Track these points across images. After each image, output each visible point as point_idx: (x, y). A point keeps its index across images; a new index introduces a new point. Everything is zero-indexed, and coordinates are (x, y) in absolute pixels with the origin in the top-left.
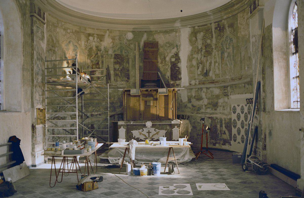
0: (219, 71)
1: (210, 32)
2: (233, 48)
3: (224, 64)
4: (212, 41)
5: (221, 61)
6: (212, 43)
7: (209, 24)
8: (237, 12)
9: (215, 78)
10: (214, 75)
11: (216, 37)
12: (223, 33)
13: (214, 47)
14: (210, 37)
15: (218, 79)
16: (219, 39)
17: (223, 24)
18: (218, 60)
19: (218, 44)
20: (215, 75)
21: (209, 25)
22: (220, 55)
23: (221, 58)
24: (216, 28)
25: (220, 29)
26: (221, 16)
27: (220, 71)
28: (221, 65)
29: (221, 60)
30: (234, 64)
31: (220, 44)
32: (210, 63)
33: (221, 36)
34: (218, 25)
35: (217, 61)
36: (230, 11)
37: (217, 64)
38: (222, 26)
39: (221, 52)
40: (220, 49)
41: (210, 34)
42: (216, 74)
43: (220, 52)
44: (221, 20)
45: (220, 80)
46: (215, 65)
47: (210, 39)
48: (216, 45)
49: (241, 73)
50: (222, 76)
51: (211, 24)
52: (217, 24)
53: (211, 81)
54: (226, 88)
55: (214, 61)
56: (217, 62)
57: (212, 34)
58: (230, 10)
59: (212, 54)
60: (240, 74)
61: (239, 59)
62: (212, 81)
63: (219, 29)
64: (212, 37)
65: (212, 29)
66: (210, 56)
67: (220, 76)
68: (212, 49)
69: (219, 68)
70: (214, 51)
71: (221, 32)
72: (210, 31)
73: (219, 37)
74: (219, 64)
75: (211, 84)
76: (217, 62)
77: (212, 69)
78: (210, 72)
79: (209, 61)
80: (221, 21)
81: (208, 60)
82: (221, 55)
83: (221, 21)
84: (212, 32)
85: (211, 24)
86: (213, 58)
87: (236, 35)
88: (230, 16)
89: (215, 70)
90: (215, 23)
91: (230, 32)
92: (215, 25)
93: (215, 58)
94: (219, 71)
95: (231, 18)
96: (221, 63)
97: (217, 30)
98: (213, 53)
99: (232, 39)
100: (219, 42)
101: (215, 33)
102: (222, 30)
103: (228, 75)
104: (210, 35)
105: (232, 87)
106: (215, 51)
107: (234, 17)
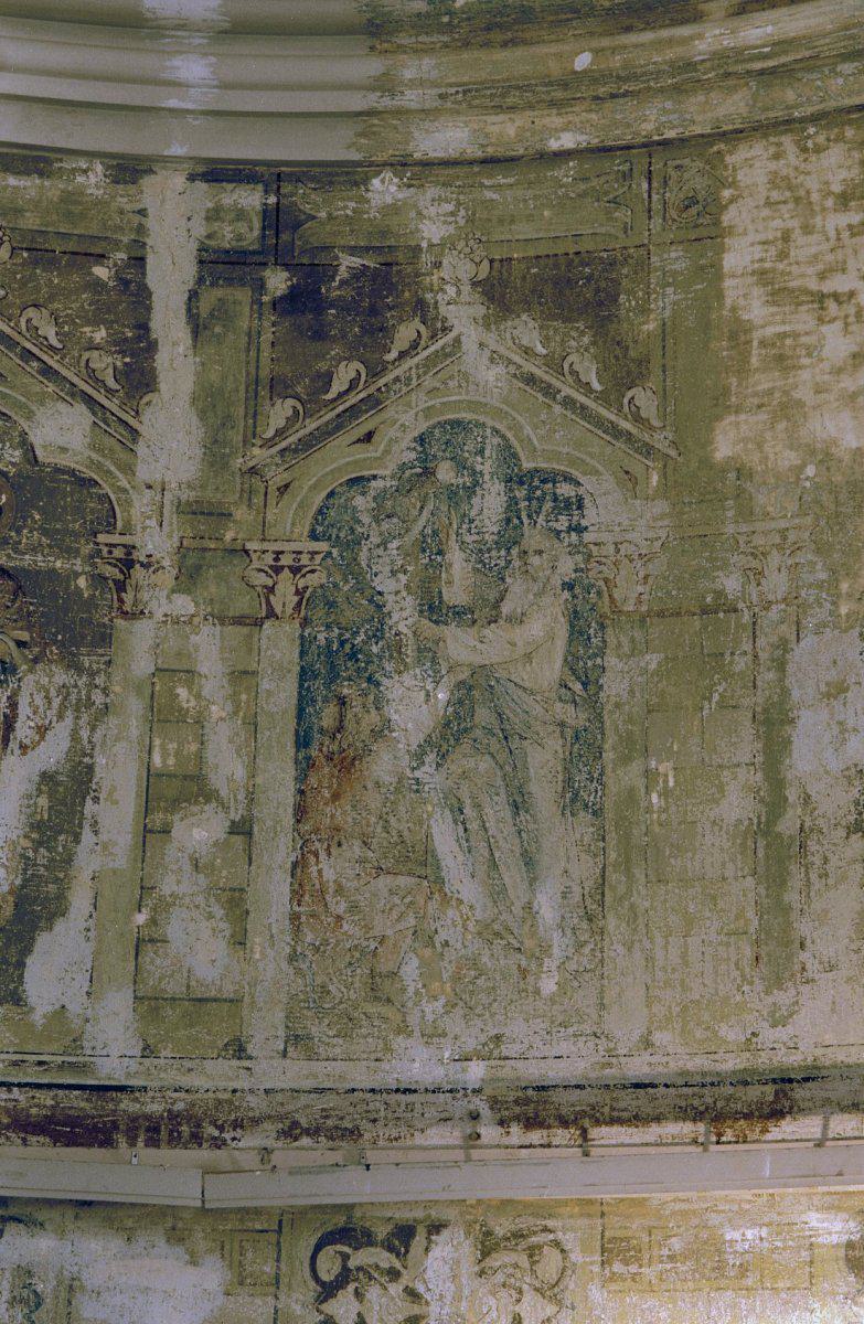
0: (240, 941)
1: (97, 285)
2: (574, 616)
3: (357, 849)
4: (135, 433)
5: (287, 796)
6: (129, 469)
7: (90, 155)
8: (733, 106)
9: (148, 1051)
10: (119, 1002)
11: (208, 401)
12: (376, 370)
13: (157, 541)
14: (104, 363)
15: (213, 1077)
16: (280, 433)
17: (384, 234)
18: (226, 766)
19: (240, 513)
20: (150, 1004)
21: (94, 181)
22: (281, 694)
23: (302, 741)
24: (219, 264)
25: (301, 302)
26: (372, 100)
27: (257, 941)
28: (278, 851)
29: (305, 767)
30: (584, 870)
31: (290, 523)
32: (47, 778)
33: (310, 404)
34: (275, 219)
35: (217, 781)
36: (583, 61)
37: (199, 832)
38: (353, 250)
39: (305, 645)
40: (285, 596)
41: (95, 322)
42: (173, 987)
43: (280, 645)
44: (356, 156)
45: (257, 1104)
46: (151, 834)
47: (89, 401)
48: (203, 513)
49: (769, 1035)
50: (297, 1040)
51: (128, 170)
52: (251, 199)
53: (46, 1099)
54: (359, 1258)
55: (151, 776)
56: (209, 795)
57: (143, 327)
58: (596, 52)
59: (104, 638)
60: (731, 1033)
61: (737, 804)
62: (77, 1102)
63: (278, 282)
64: (139, 379)
65: (139, 261)
66: (61, 676)
67: (264, 1030)
68: (128, 564)
69: (236, 903)
70: (162, 598)
71: (319, 335)
72: (101, 272)
73: (279, 413)
74: (242, 829)
75: (39, 1147)
76: (209, 795)
77: (80, 900)
78: (43, 940)
79: (53, 753)
80: (345, 176)
81: (23, 730)
82: (304, 702)
83: (345, 176)
84: (134, 290)
85: (128, 170)
86: (135, 706)
87: (660, 441)
88: (567, 141)
89: (141, 918)
90: (216, 173)
91: (531, 380)
92: (214, 215)
93: (161, 715)
94: (240, 941)
95: (566, 173)
96: (300, 813)
97: (243, 295)
98: (139, 646)
99: (565, 490)
100: (277, 477)
101: (197, 327)
102: (345, 307)
103: (432, 1035)
104: (100, 335)
105: (533, 1252)
106: (184, 605)
107: (627, 176)
